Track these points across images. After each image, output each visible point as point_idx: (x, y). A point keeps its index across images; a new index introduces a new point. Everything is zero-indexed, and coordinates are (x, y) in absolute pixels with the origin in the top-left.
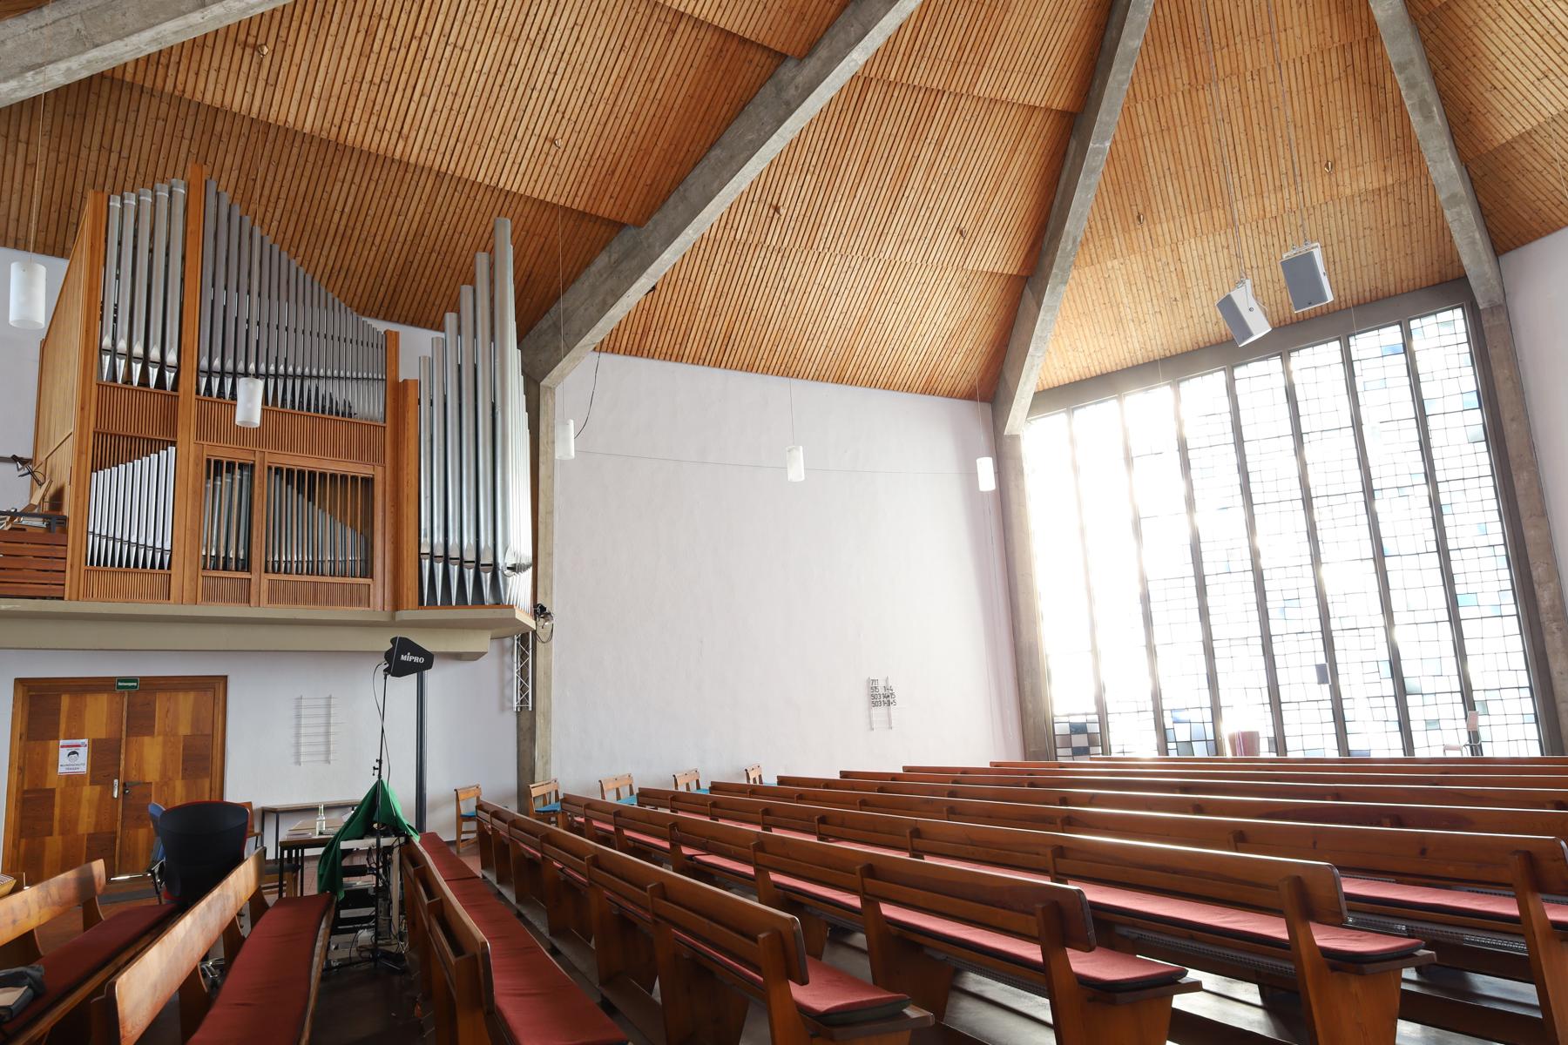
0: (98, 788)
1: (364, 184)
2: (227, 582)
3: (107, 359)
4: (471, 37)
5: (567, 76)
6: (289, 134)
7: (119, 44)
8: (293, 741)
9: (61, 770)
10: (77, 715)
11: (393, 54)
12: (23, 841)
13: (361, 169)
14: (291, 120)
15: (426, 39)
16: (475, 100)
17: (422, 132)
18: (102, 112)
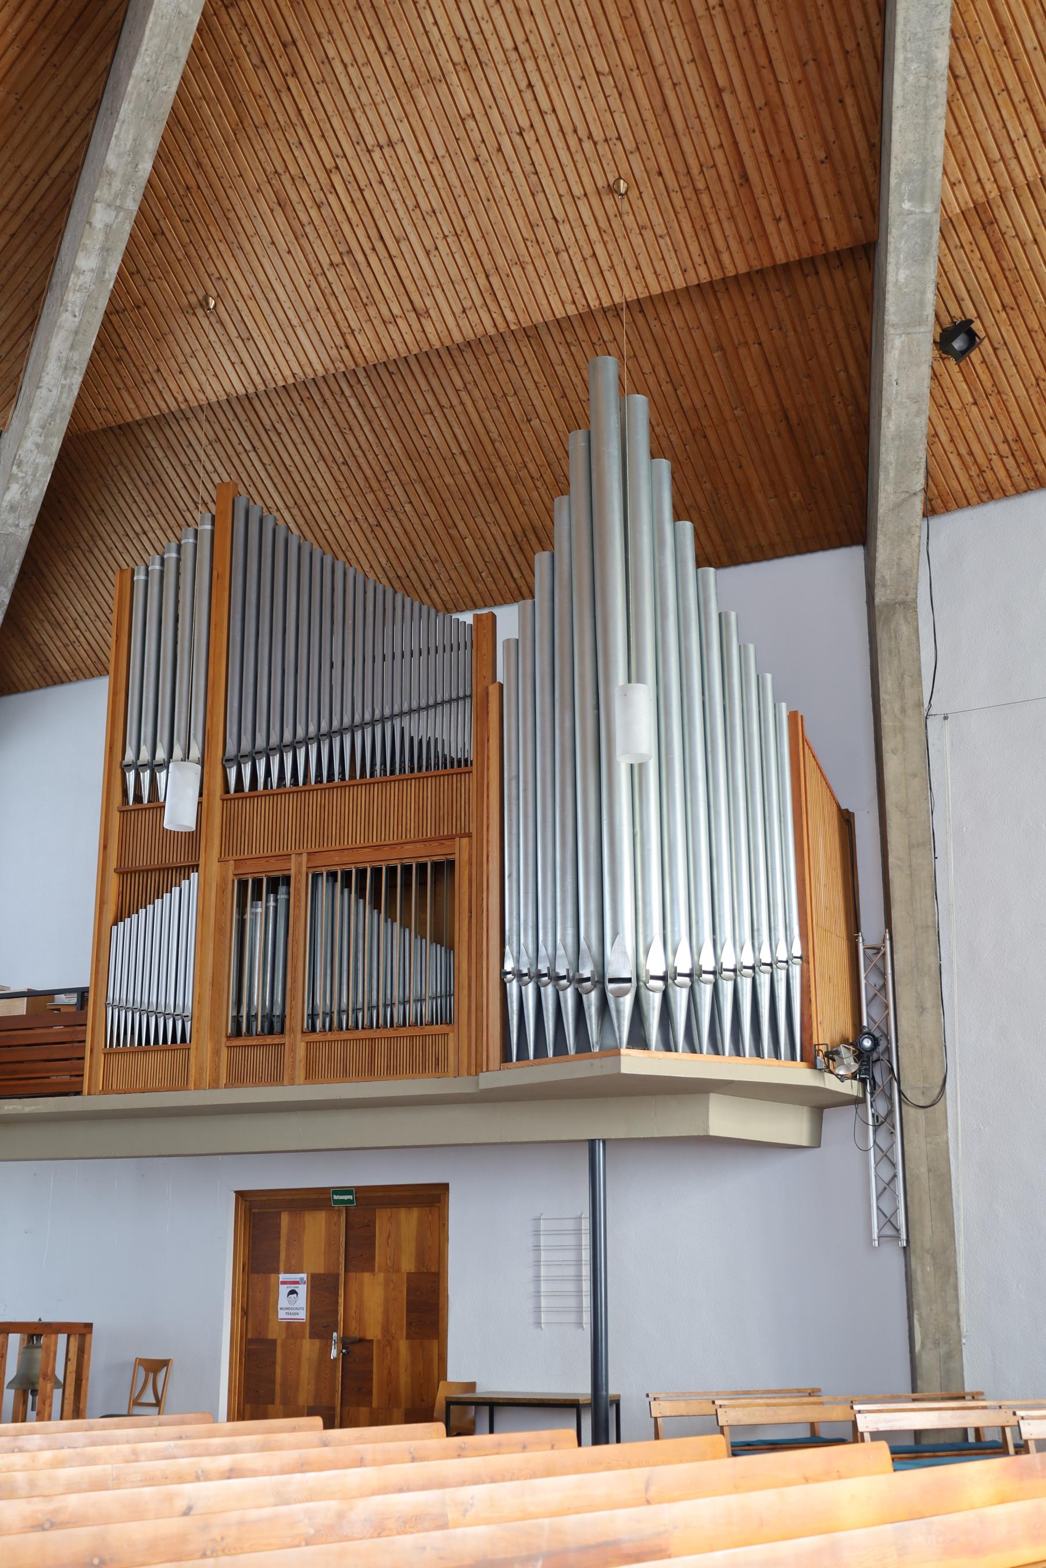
0: (317, 1342)
1: (455, 402)
2: (259, 1052)
3: (131, 776)
4: (388, 120)
5: (549, 78)
6: (300, 390)
7: (43, 392)
8: (531, 1288)
9: (282, 1314)
10: (296, 1236)
11: (326, 210)
12: (248, 1406)
13: (434, 382)
14: (297, 370)
15: (342, 163)
16: (462, 202)
17: (437, 292)
18: (166, 463)
